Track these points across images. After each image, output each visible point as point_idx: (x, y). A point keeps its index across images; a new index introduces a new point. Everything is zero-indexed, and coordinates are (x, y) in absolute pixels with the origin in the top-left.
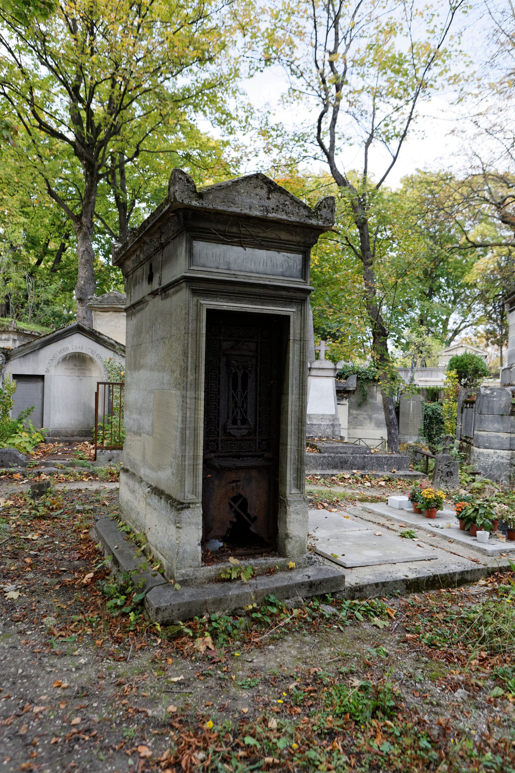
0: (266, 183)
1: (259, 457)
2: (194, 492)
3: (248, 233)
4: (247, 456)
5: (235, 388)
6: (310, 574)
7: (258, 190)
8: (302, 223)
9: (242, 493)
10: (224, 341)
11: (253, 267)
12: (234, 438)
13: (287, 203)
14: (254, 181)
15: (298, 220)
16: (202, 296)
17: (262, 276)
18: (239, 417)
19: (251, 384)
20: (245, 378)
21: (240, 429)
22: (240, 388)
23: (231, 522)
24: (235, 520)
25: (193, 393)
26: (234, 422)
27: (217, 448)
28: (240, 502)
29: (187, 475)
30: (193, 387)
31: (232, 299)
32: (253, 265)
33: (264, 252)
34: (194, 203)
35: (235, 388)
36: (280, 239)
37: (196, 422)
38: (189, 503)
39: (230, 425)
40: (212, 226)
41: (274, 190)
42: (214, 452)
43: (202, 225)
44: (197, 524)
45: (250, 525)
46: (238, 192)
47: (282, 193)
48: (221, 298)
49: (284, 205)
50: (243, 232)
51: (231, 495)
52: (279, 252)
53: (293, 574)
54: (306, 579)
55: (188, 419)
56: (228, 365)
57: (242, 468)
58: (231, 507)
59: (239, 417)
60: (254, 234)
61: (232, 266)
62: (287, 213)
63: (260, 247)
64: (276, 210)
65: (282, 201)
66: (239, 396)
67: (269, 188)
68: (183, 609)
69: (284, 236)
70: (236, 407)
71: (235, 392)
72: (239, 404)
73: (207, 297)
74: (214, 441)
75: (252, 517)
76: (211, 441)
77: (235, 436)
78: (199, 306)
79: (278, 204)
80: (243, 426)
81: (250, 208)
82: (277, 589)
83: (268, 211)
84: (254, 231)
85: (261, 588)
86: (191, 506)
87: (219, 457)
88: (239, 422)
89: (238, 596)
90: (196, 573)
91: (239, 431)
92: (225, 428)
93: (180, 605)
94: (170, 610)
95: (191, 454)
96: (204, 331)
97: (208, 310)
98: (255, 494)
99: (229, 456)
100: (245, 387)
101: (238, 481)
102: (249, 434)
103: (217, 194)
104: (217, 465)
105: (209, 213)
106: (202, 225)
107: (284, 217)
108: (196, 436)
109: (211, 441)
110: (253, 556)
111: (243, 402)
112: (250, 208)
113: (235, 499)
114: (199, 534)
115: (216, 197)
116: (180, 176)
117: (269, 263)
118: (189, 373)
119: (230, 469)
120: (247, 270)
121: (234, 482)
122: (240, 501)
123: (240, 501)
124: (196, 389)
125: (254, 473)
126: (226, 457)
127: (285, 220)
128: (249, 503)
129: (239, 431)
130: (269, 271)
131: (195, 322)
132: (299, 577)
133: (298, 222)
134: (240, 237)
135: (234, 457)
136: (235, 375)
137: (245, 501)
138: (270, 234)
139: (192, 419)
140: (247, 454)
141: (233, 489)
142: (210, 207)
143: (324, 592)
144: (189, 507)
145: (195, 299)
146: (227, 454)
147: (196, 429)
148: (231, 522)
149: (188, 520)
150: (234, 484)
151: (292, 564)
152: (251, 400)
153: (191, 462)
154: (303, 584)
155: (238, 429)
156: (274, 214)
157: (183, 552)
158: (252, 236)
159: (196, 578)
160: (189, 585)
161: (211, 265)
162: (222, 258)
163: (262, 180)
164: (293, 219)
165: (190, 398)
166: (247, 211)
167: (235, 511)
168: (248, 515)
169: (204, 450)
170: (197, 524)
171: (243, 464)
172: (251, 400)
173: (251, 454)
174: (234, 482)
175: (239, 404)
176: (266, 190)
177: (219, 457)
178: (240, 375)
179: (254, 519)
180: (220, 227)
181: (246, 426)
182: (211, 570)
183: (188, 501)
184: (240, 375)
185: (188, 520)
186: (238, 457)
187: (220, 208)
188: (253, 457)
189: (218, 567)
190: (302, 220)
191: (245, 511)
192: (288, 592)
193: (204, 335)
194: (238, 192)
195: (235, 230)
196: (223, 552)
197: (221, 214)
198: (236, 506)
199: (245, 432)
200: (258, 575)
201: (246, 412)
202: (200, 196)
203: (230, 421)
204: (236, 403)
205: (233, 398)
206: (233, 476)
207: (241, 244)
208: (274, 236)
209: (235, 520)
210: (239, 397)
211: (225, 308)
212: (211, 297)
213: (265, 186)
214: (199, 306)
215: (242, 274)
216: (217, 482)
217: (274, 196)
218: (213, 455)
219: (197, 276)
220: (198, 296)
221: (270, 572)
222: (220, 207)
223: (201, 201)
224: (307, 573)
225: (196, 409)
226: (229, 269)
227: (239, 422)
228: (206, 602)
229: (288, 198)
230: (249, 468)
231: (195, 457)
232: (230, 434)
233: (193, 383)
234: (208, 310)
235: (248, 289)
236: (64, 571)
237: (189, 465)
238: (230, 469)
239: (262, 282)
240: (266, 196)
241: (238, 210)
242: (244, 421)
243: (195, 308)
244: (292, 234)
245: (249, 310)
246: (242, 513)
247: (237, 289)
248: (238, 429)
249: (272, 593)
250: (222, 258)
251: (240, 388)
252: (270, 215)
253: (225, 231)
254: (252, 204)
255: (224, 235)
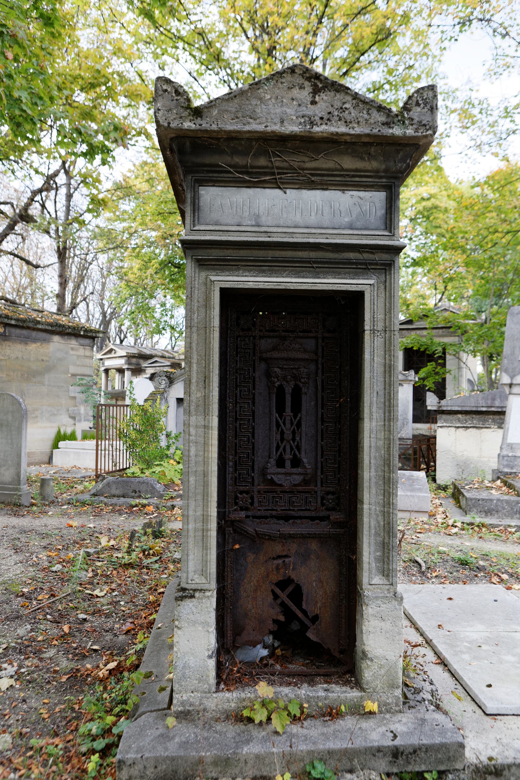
0: (309, 79)
1: (322, 519)
2: (203, 573)
3: (285, 165)
4: (300, 518)
5: (280, 410)
6: (399, 728)
7: (296, 92)
8: (375, 136)
9: (293, 576)
10: (261, 337)
11: (298, 219)
12: (279, 489)
13: (347, 106)
14: (288, 77)
15: (367, 131)
16: (214, 270)
17: (313, 231)
18: (288, 456)
19: (308, 403)
20: (297, 394)
21: (290, 474)
22: (288, 409)
23: (275, 621)
24: (282, 618)
25: (201, 418)
26: (280, 463)
27: (252, 504)
28: (290, 591)
29: (191, 546)
30: (201, 409)
31: (263, 271)
32: (298, 215)
33: (318, 194)
34: (188, 125)
35: (280, 410)
36: (343, 169)
37: (206, 462)
38: (195, 590)
39: (272, 468)
40: (222, 161)
41: (324, 88)
42: (247, 509)
43: (208, 160)
44: (206, 624)
45: (307, 628)
46: (261, 99)
47: (337, 91)
48: (244, 271)
49: (342, 110)
50: (277, 164)
51: (276, 578)
52: (343, 191)
53: (366, 724)
54: (388, 742)
55: (193, 458)
56: (268, 375)
57: (291, 536)
58: (276, 597)
59: (288, 456)
60: (296, 165)
61: (263, 220)
62: (347, 123)
63: (311, 185)
64: (327, 119)
65: (338, 104)
66: (288, 422)
67: (315, 86)
68: (163, 767)
69: (348, 163)
70: (282, 439)
71: (281, 416)
72: (288, 435)
73: (223, 270)
74: (247, 492)
75: (310, 615)
76: (241, 493)
77: (281, 485)
78: (208, 285)
79: (331, 109)
80: (294, 470)
81: (282, 122)
82: (331, 753)
83: (312, 123)
84: (295, 160)
85: (303, 747)
86: (197, 594)
87: (254, 517)
88: (288, 464)
89: (257, 757)
90: (205, 701)
91: (287, 478)
92: (264, 472)
93: (157, 762)
94: (141, 767)
95: (199, 513)
96: (216, 322)
97: (222, 290)
98: (315, 579)
99: (272, 517)
100: (297, 408)
101: (286, 556)
102: (305, 482)
103: (225, 106)
104: (250, 530)
105: (218, 139)
106: (208, 160)
107: (343, 129)
108: (206, 485)
109: (241, 493)
110: (309, 678)
111: (294, 433)
112: (282, 122)
113: (283, 584)
114: (210, 640)
115: (222, 112)
116: (165, 87)
117: (326, 210)
118: (193, 387)
119: (271, 538)
120: (289, 223)
121: (279, 557)
122: (290, 589)
123: (290, 589)
124: (206, 413)
125: (314, 546)
126: (266, 517)
127: (344, 134)
128: (305, 591)
129: (287, 478)
130: (326, 224)
131: (203, 310)
132: (376, 734)
133: (368, 135)
134: (273, 174)
135: (278, 518)
136: (281, 390)
137: (298, 589)
138: (324, 163)
139: (201, 459)
140: (301, 514)
141: (278, 568)
142: (214, 127)
143: (423, 768)
144: (192, 597)
145: (203, 274)
146: (268, 513)
147: (205, 474)
148: (275, 621)
149: (191, 617)
150: (280, 561)
151: (371, 706)
152: (307, 428)
153: (199, 525)
154: (379, 750)
155: (286, 474)
156: (324, 127)
157: (184, 667)
158: (292, 168)
159: (205, 710)
160: (193, 720)
161: (229, 221)
162: (246, 208)
163: (302, 75)
164: (358, 130)
165: (197, 427)
166: (276, 128)
167: (283, 605)
168: (305, 612)
169: (218, 507)
170: (206, 624)
171: (293, 530)
172: (307, 428)
173: (307, 514)
174: (279, 557)
175: (288, 435)
176: (308, 89)
177: (254, 517)
178: (288, 390)
179: (315, 619)
180: (238, 160)
181: (300, 470)
182: (230, 698)
183: (193, 587)
184: (288, 390)
185: (191, 617)
186: (287, 518)
187: (230, 127)
188: (313, 519)
189: (243, 695)
190: (375, 131)
191: (299, 606)
192: (351, 760)
193: (217, 330)
194: (261, 99)
195: (262, 162)
196: (266, 665)
197: (236, 139)
198: (283, 596)
199: (298, 479)
200: (309, 716)
201: (298, 448)
202: (198, 112)
203: (273, 461)
204: (282, 433)
205: (278, 425)
206: (278, 549)
207: (277, 184)
208: (330, 165)
209: (282, 618)
210: (288, 425)
211: (251, 285)
212: (229, 270)
213: (307, 84)
214: (208, 285)
215: (280, 230)
216: (251, 557)
217: (325, 100)
218: (243, 514)
219: (203, 238)
220: (208, 269)
221: (332, 713)
222: (231, 126)
223: (199, 121)
224: (393, 727)
225: (206, 444)
226: (259, 226)
227: (288, 464)
228: (201, 761)
229: (349, 98)
230: (304, 537)
231: (205, 518)
232: (272, 482)
233: (201, 402)
234: (222, 290)
235: (289, 254)
236: (95, 651)
237: (195, 530)
238: (271, 538)
239: (312, 240)
240: (309, 99)
241: (261, 128)
242: (296, 462)
243: (203, 289)
244: (362, 159)
245: (292, 287)
246: (294, 608)
247: (270, 254)
248: (286, 474)
249: (321, 760)
250: (246, 208)
251: (288, 409)
252: (316, 129)
253: (246, 166)
254: (284, 115)
255: (248, 173)
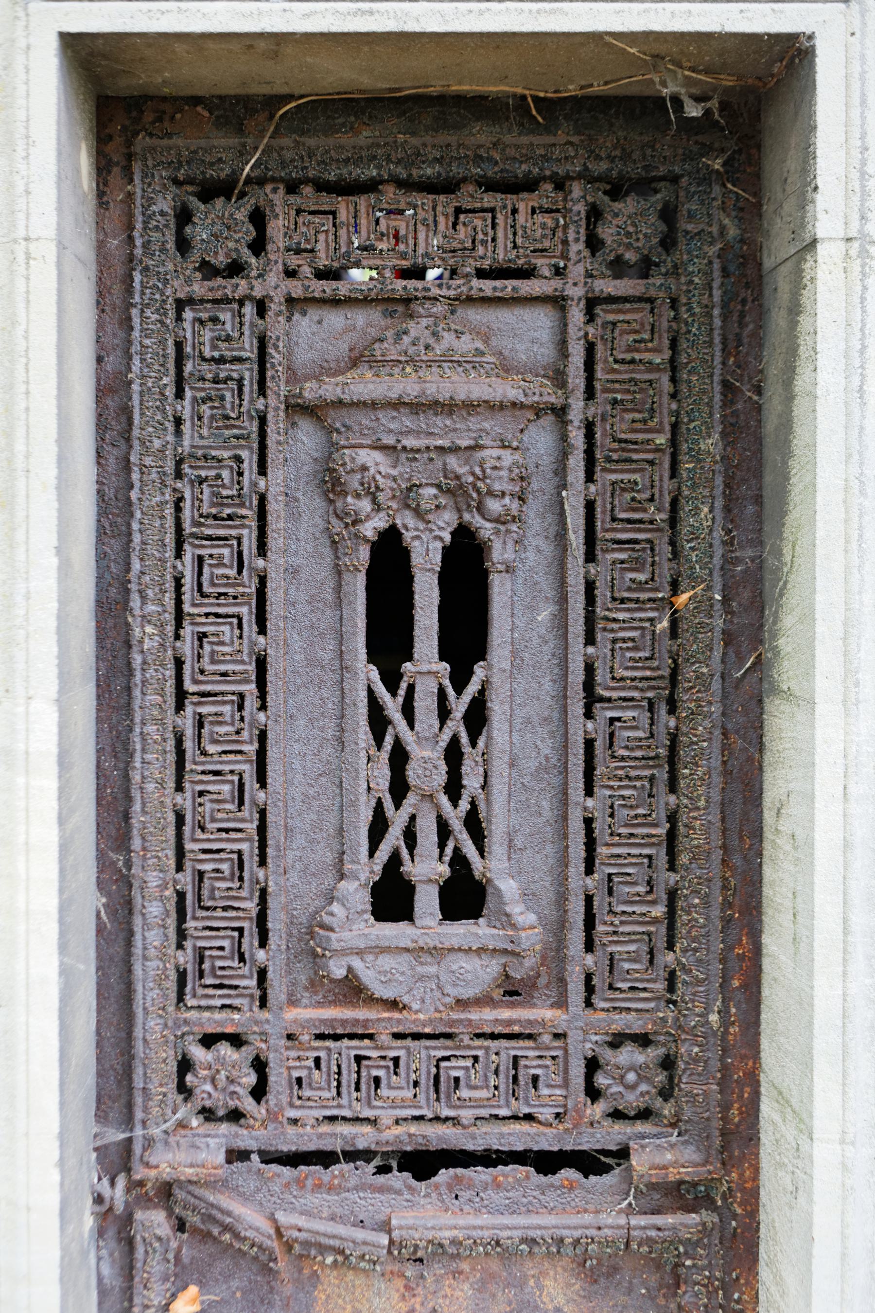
1: (589, 1163)
4: (490, 1159)
18: (427, 869)
19: (518, 611)
20: (466, 567)
26: (392, 899)
35: (389, 642)
56: (331, 484)
59: (427, 869)
66: (425, 706)
70: (399, 788)
71: (391, 680)
72: (427, 766)
76: (209, 1041)
77: (394, 1005)
80: (460, 931)
87: (269, 1158)
88: (427, 901)
91: (428, 967)
100: (466, 638)
104: (251, 1218)
109: (209, 1041)
111: (453, 755)
155: (418, 951)
175: (427, 766)
186: (422, 1164)
188: (546, 1162)
199: (481, 974)
203: (356, 893)
204: (399, 758)
205: (378, 722)
227: (427, 901)
232: (352, 990)
242: (464, 896)
